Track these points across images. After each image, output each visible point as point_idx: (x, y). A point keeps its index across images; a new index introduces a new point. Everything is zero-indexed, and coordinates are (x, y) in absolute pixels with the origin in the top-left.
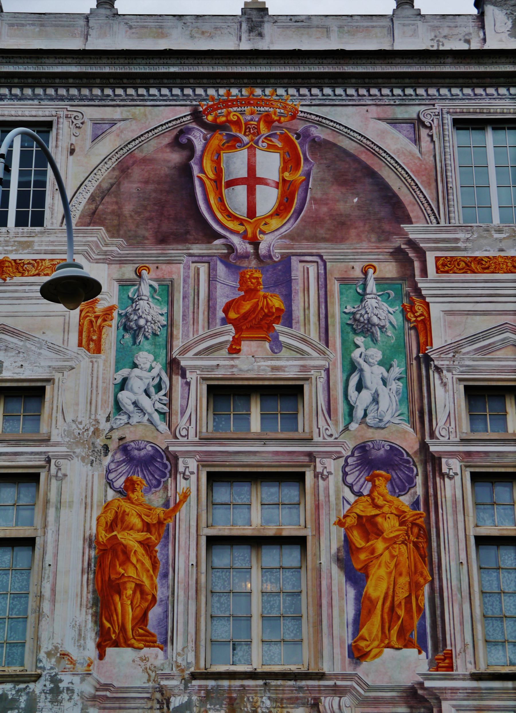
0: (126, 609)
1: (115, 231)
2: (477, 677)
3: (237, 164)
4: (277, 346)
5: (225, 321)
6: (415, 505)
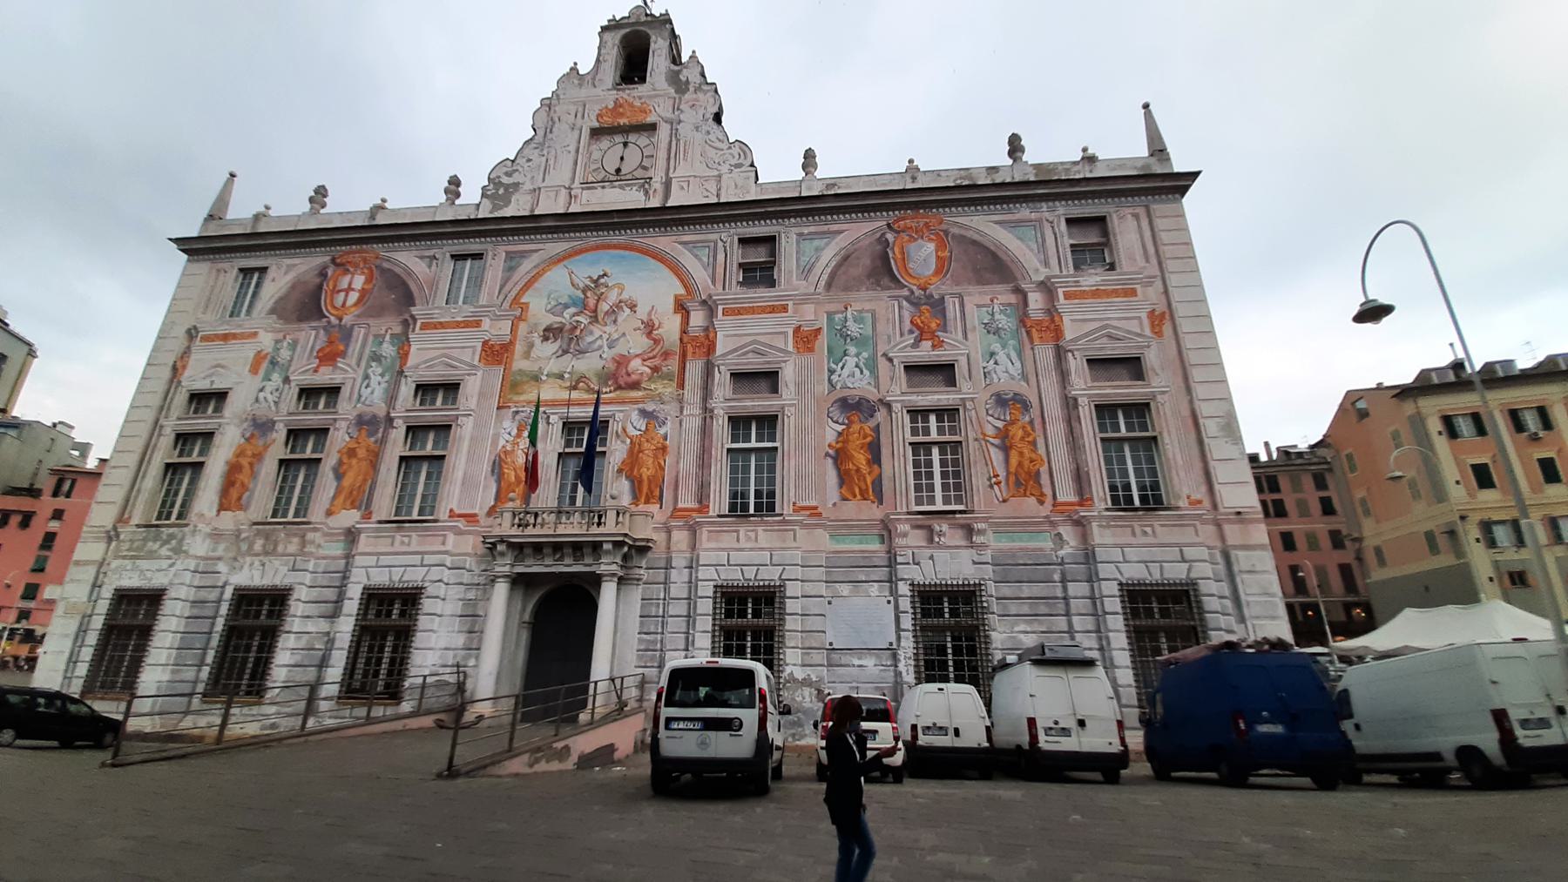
0: (234, 493)
1: (280, 317)
2: (380, 522)
3: (347, 279)
4: (335, 367)
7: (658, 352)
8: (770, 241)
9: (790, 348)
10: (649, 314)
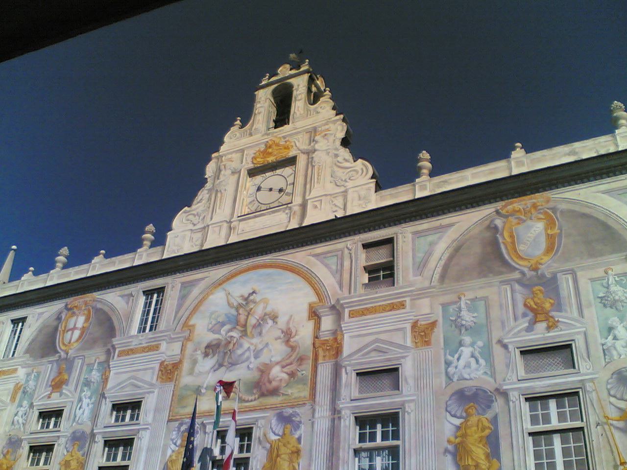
5: (50, 386)
6: (83, 455)
7: (295, 358)
8: (389, 241)
9: (409, 343)
10: (288, 323)
